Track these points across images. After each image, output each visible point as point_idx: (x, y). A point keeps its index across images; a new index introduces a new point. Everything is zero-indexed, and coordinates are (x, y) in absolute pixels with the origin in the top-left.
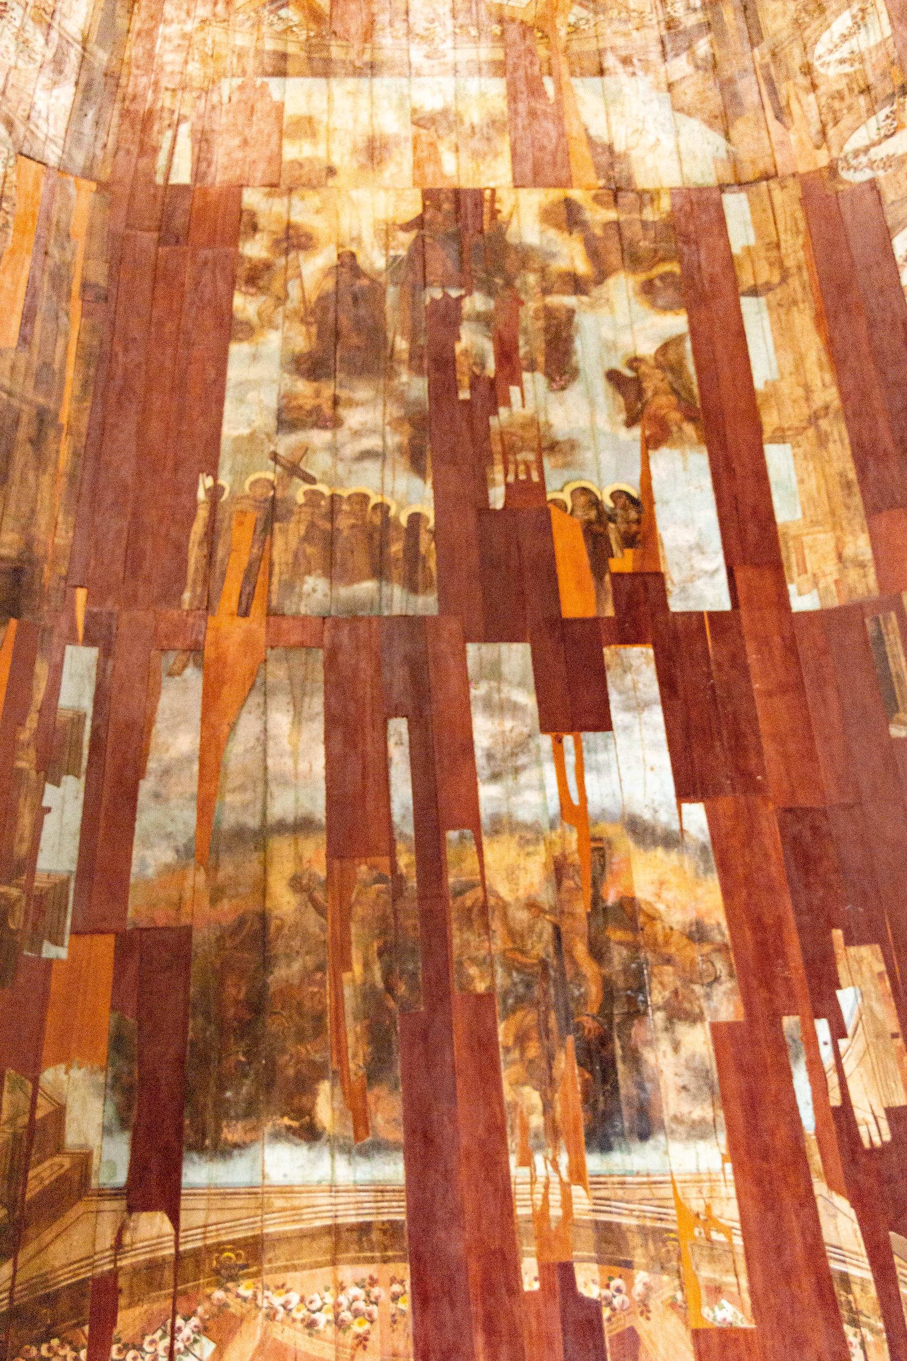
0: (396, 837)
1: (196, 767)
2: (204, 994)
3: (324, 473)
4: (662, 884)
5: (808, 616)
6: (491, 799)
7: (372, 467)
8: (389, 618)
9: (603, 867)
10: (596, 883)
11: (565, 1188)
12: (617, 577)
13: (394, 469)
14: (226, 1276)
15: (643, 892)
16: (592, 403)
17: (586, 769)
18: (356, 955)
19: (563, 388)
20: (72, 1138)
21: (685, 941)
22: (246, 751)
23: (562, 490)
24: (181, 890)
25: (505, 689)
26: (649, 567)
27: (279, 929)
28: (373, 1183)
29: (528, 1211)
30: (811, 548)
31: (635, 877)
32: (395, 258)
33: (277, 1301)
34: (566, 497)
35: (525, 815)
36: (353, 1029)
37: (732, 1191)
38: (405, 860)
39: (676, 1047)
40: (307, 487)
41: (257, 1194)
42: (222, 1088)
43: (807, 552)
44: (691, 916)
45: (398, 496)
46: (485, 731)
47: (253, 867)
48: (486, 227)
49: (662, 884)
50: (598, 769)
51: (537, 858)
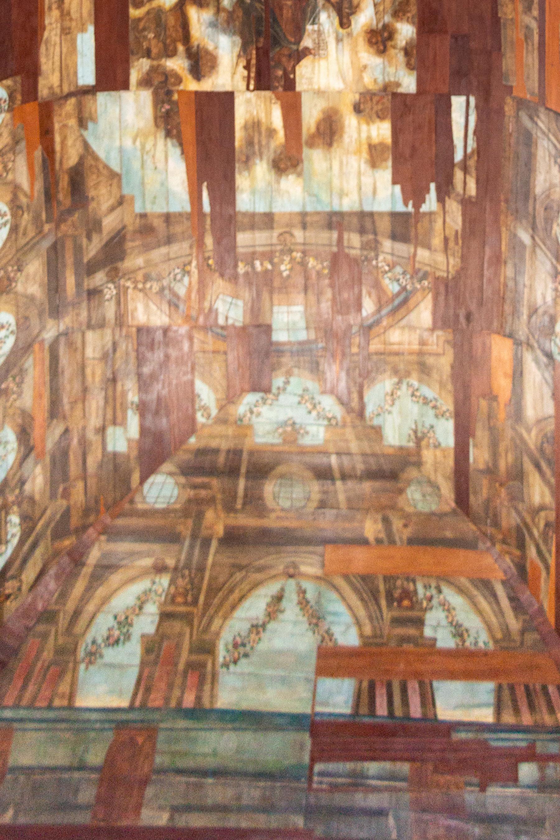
48: (254, 52)
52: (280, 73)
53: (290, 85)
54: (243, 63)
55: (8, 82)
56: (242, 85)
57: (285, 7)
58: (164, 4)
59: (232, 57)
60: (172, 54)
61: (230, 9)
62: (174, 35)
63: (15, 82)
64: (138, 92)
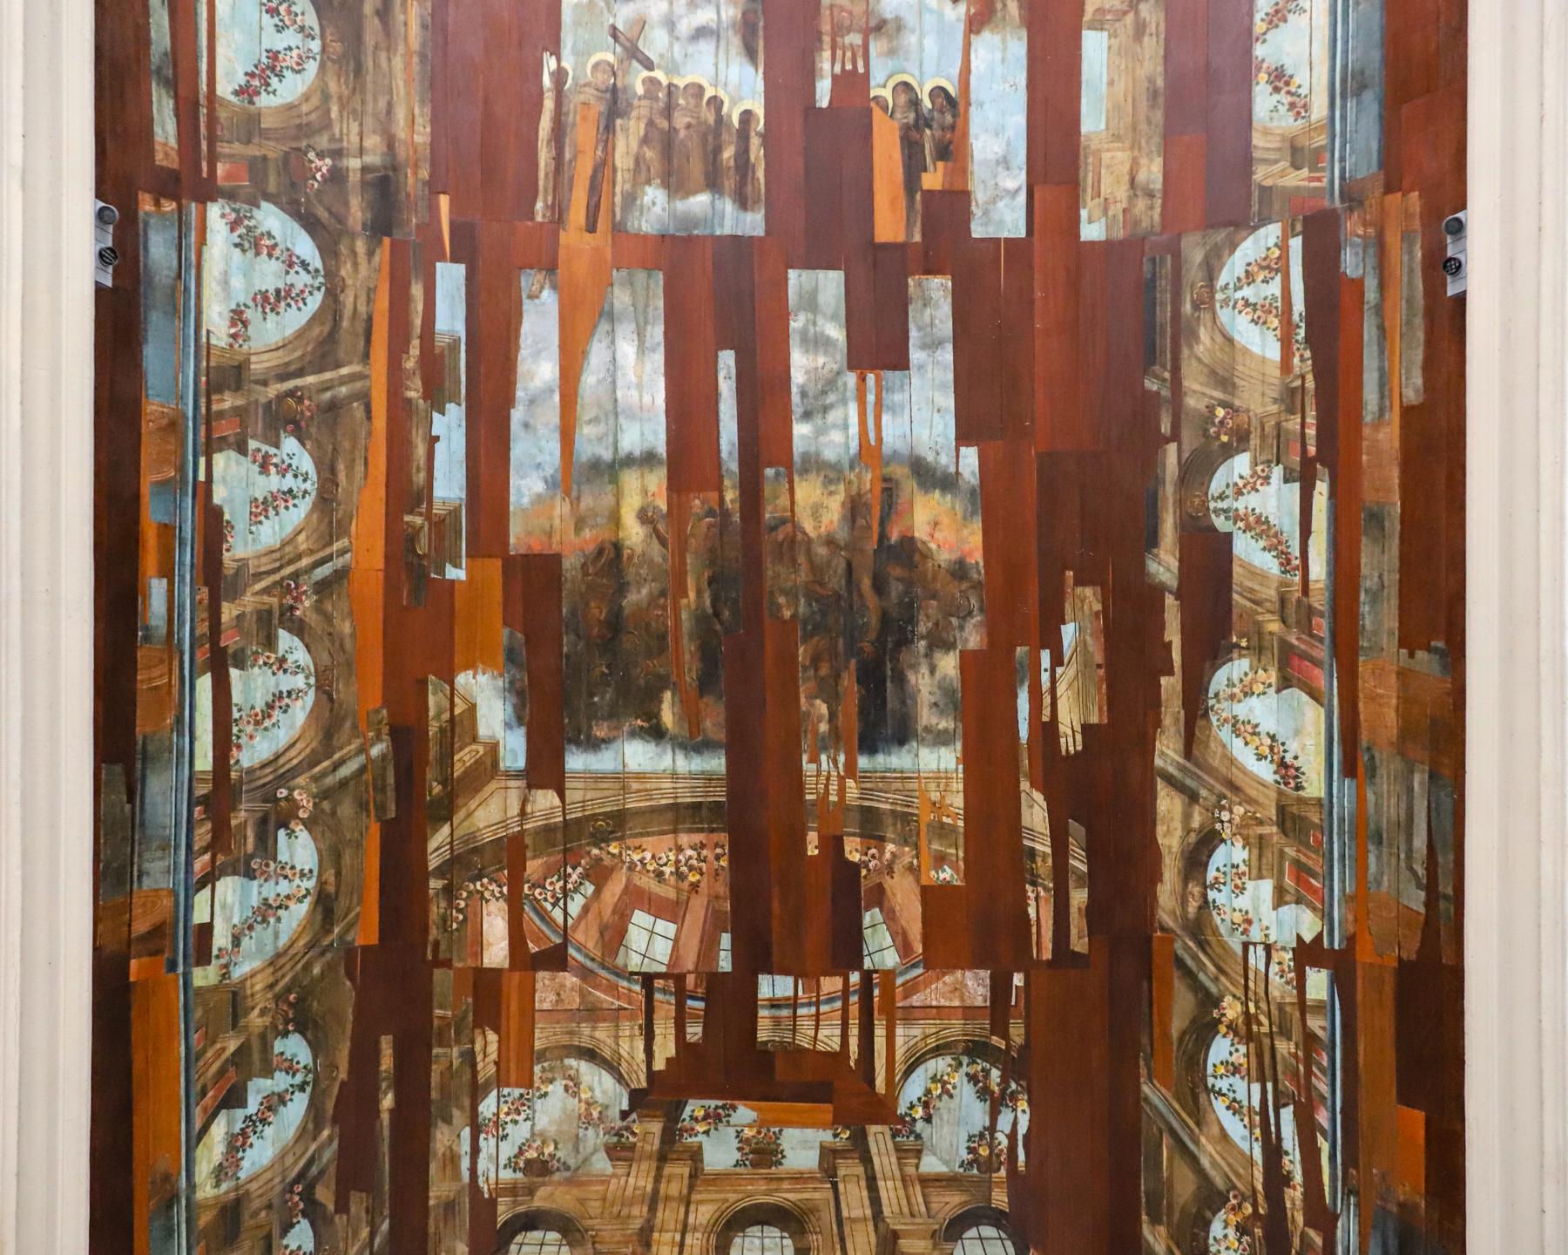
1: (557, 398)
2: (573, 612)
3: (662, 56)
4: (936, 524)
5: (1092, 244)
6: (803, 437)
7: (706, 47)
8: (720, 238)
9: (890, 507)
11: (842, 779)
12: (928, 195)
14: (601, 839)
15: (921, 532)
18: (691, 582)
20: (483, 731)
21: (949, 578)
22: (599, 382)
24: (551, 518)
25: (820, 322)
26: (958, 187)
27: (630, 558)
28: (703, 773)
29: (813, 797)
30: (1108, 167)
33: (636, 857)
34: (887, 93)
35: (829, 455)
36: (689, 647)
37: (961, 787)
38: (730, 495)
39: (933, 670)
40: (646, 73)
41: (621, 779)
42: (591, 695)
43: (1103, 171)
44: (954, 556)
45: (730, 88)
46: (802, 366)
47: (608, 500)
49: (936, 524)
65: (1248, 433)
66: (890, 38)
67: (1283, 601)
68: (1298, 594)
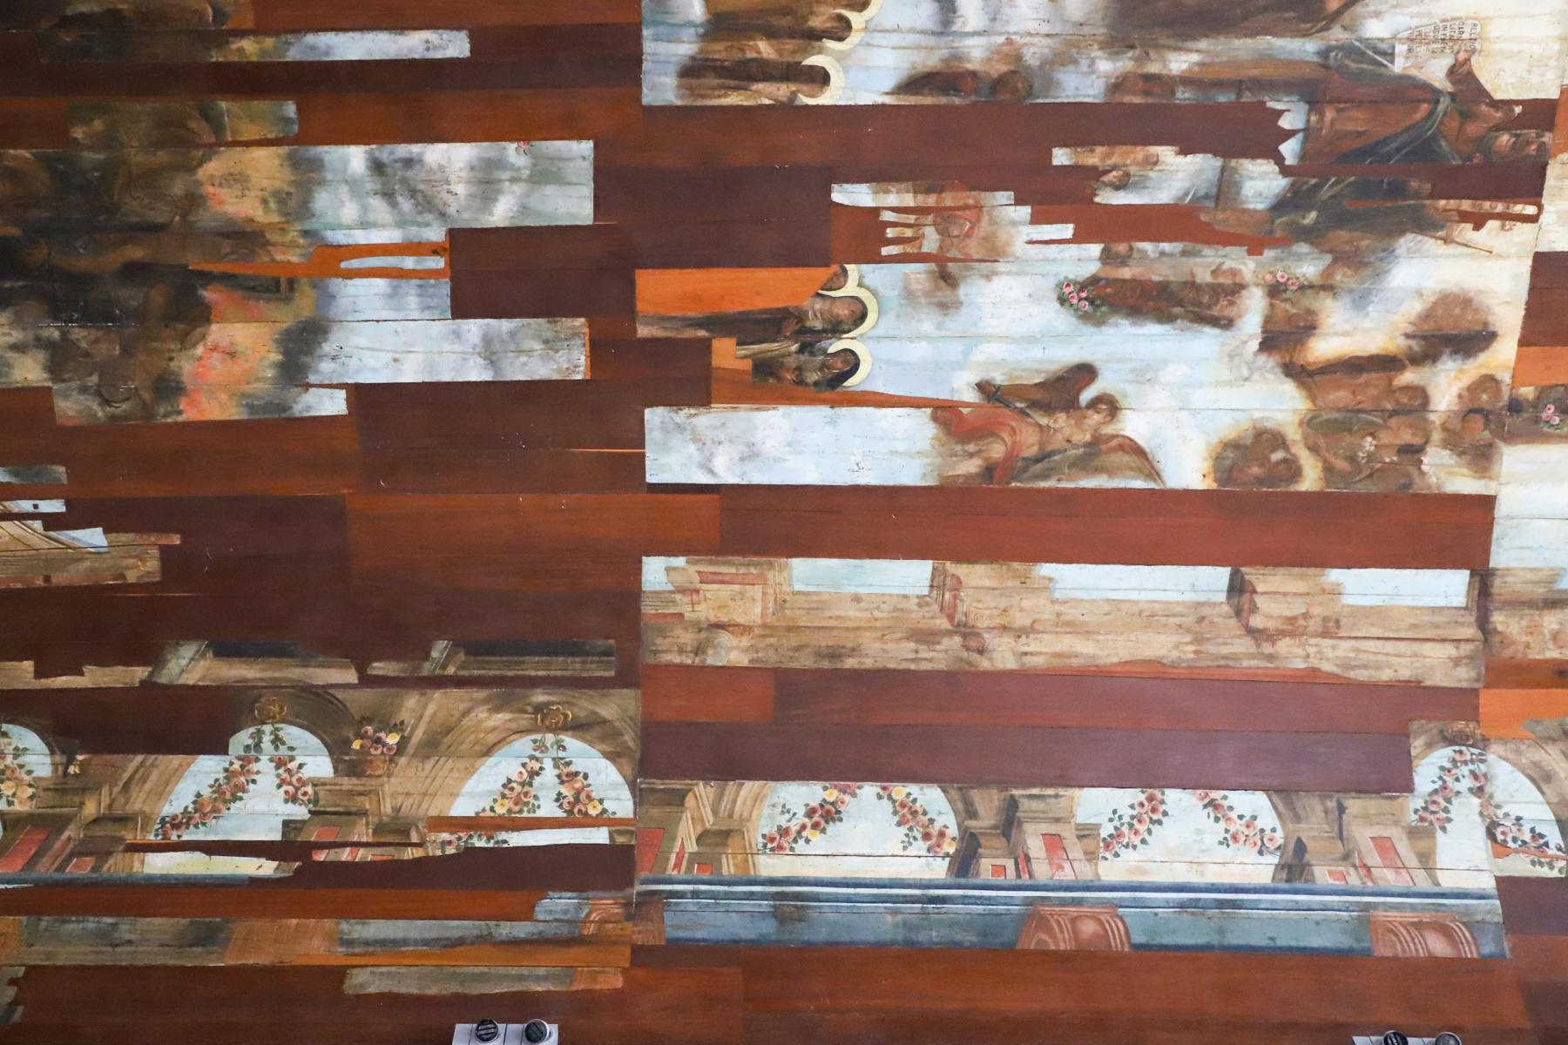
0: (283, 38)
5: (638, 571)
6: (345, 161)
9: (253, 289)
10: (228, 279)
12: (705, 347)
13: (918, 48)
15: (218, 332)
16: (1031, 339)
17: (395, 282)
19: (1062, 300)
23: (860, 285)
25: (518, 189)
31: (240, 325)
32: (1390, 55)
35: (322, 200)
38: (249, 48)
44: (185, 379)
45: (862, 52)
46: (451, 160)
48: (1442, 203)
50: (393, 295)
51: (260, 212)
52: (1505, 139)
53: (1541, 114)
54: (1466, 231)
55: (1417, 745)
56: (1523, 231)
57: (1338, 127)
58: (1295, 411)
59: (1448, 257)
60: (1421, 397)
61: (1328, 258)
62: (1374, 392)
63: (1422, 732)
64: (1502, 480)
65: (359, 775)
66: (929, 294)
67: (124, 820)
68: (129, 838)
